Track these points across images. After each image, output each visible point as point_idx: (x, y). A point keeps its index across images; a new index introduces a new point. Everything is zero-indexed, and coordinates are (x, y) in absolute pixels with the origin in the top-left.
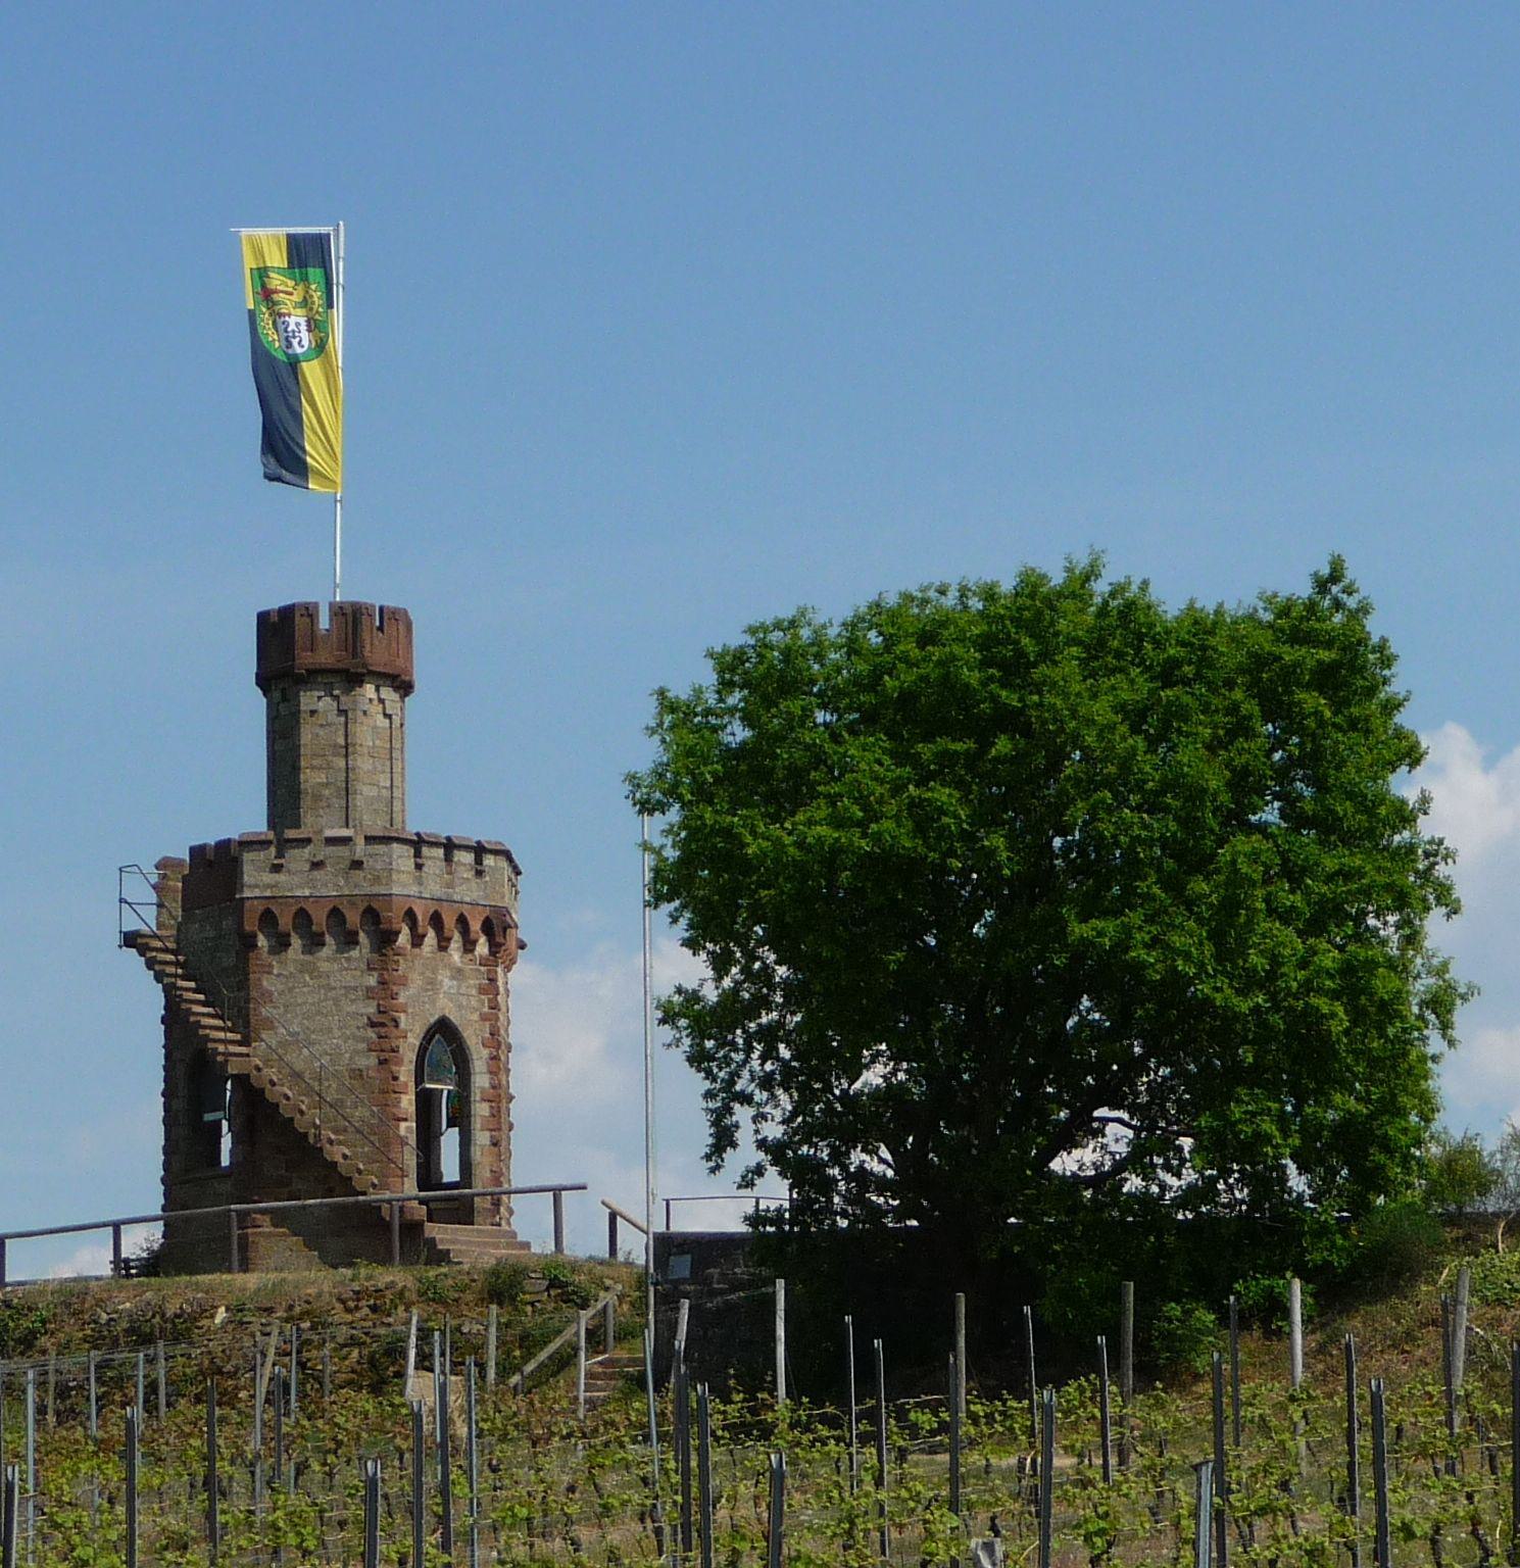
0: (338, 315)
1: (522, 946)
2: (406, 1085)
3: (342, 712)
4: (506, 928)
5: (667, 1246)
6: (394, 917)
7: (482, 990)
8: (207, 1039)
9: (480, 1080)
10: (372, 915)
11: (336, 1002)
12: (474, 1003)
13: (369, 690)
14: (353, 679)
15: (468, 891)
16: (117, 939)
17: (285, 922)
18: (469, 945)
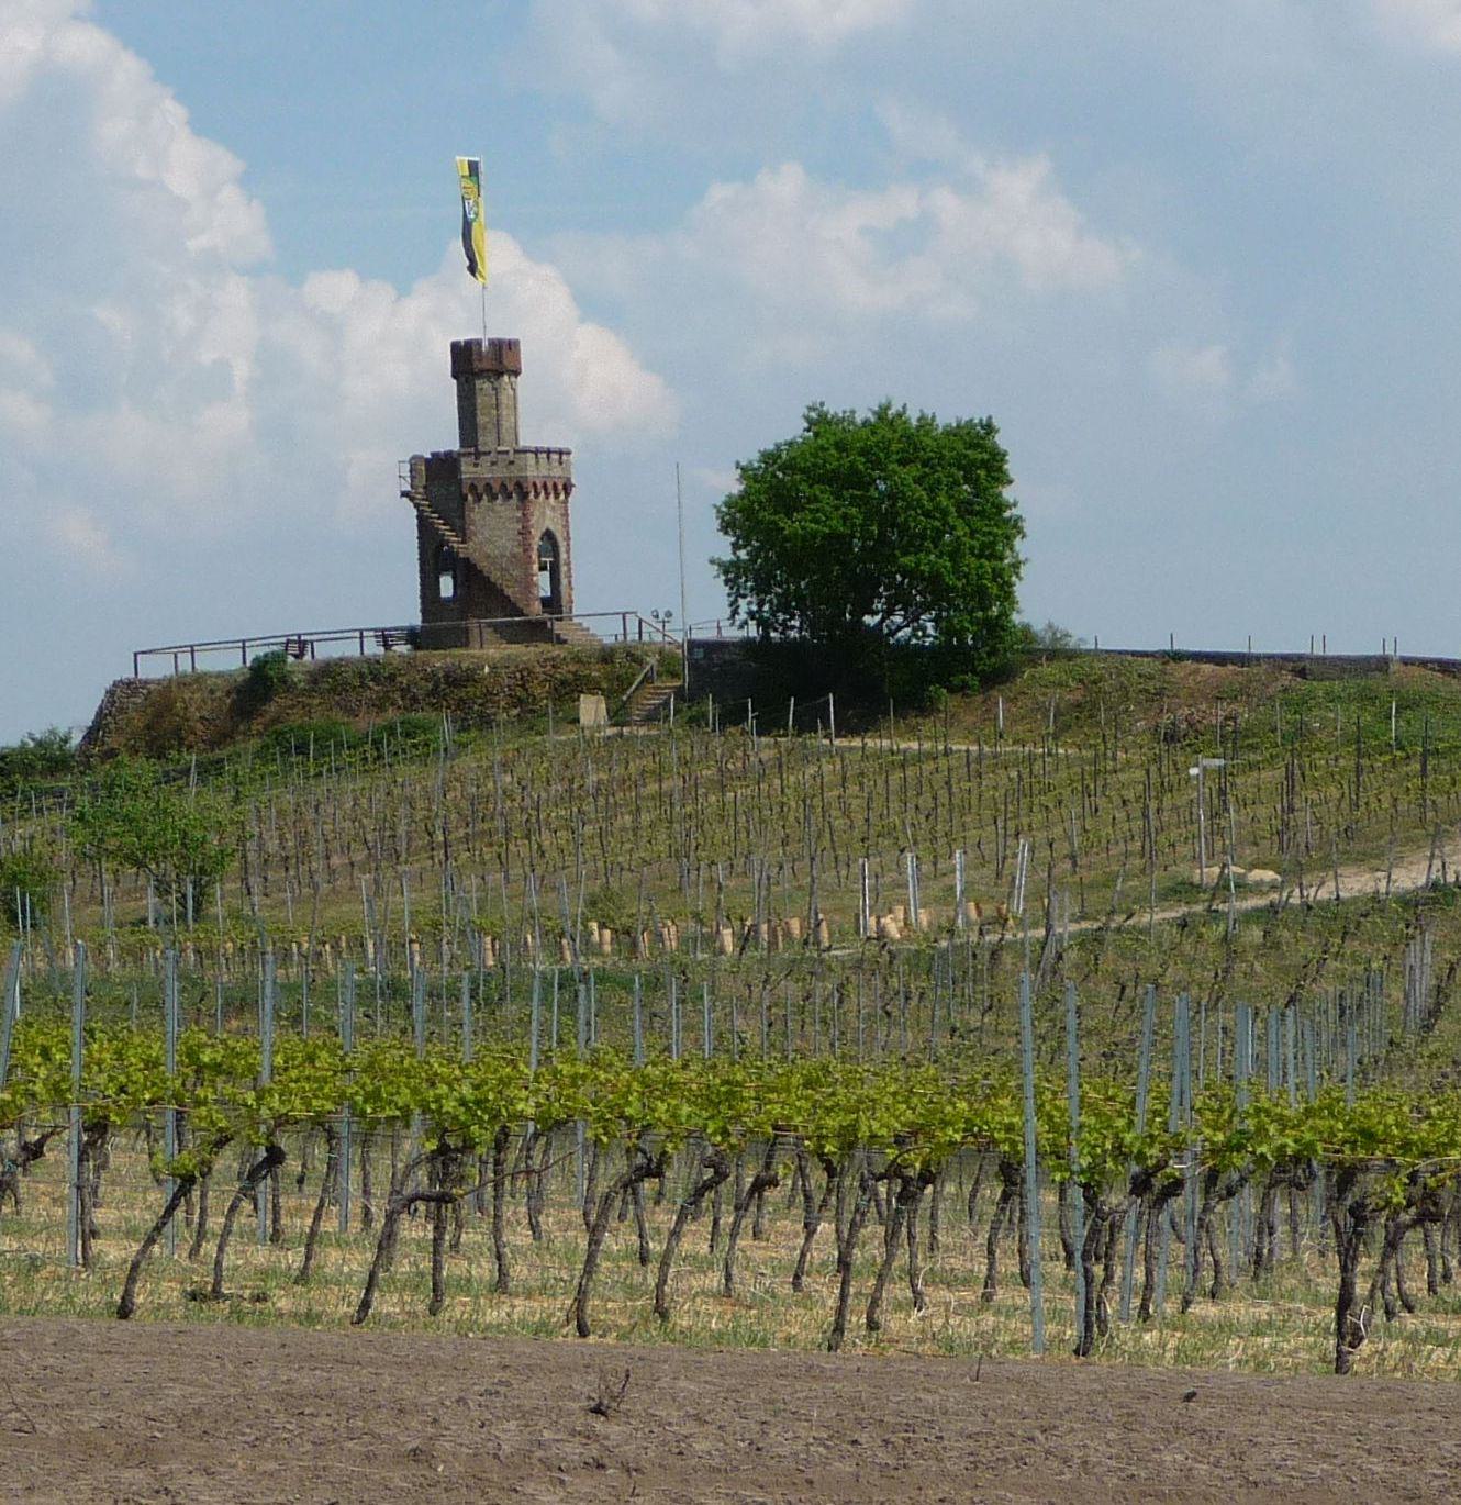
3: (495, 389)
5: (693, 645)
7: (562, 515)
9: (563, 556)
10: (519, 485)
14: (499, 374)
15: (557, 472)
17: (480, 489)
18: (557, 496)
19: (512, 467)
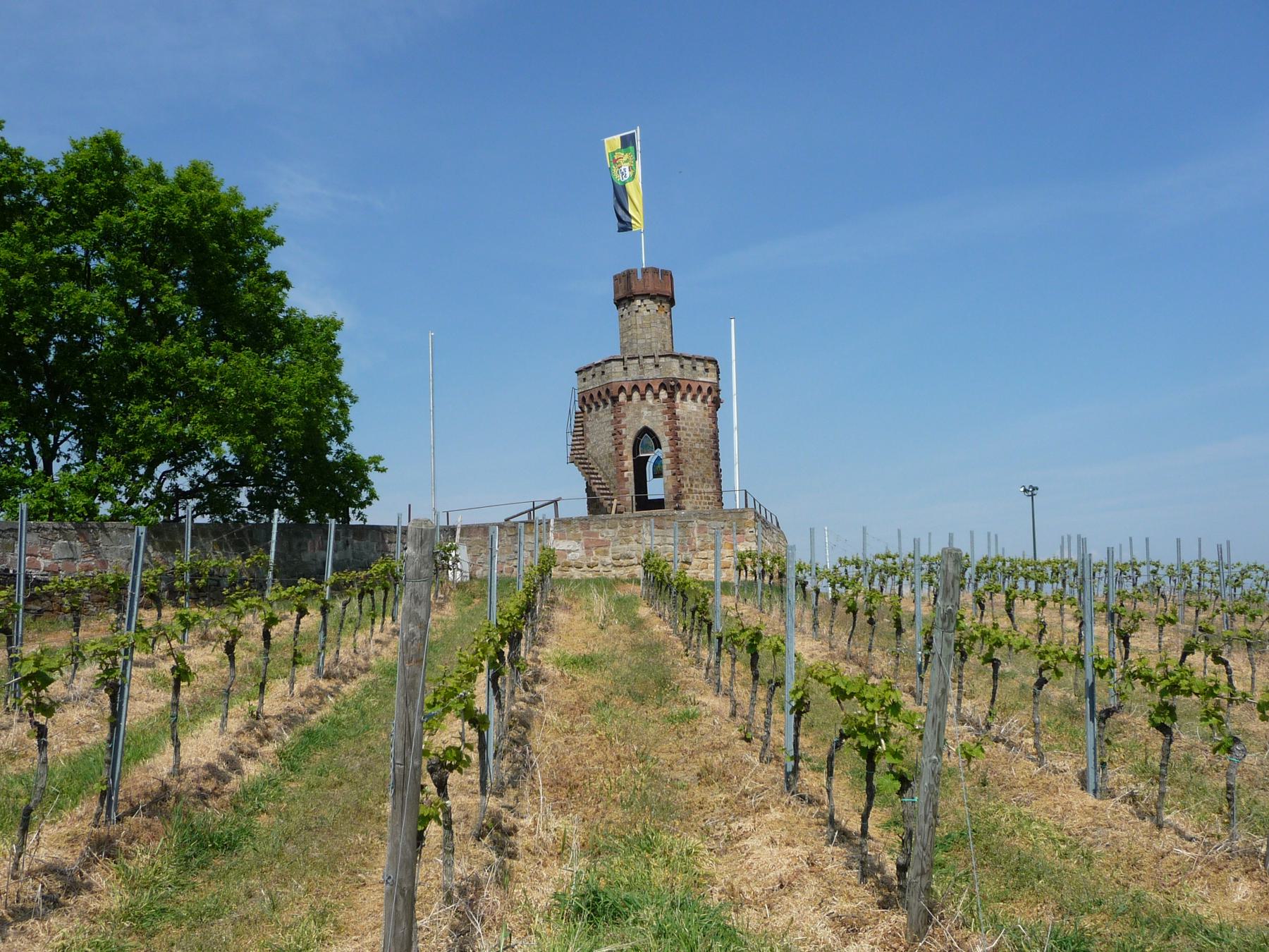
0: (638, 163)
18: (656, 396)
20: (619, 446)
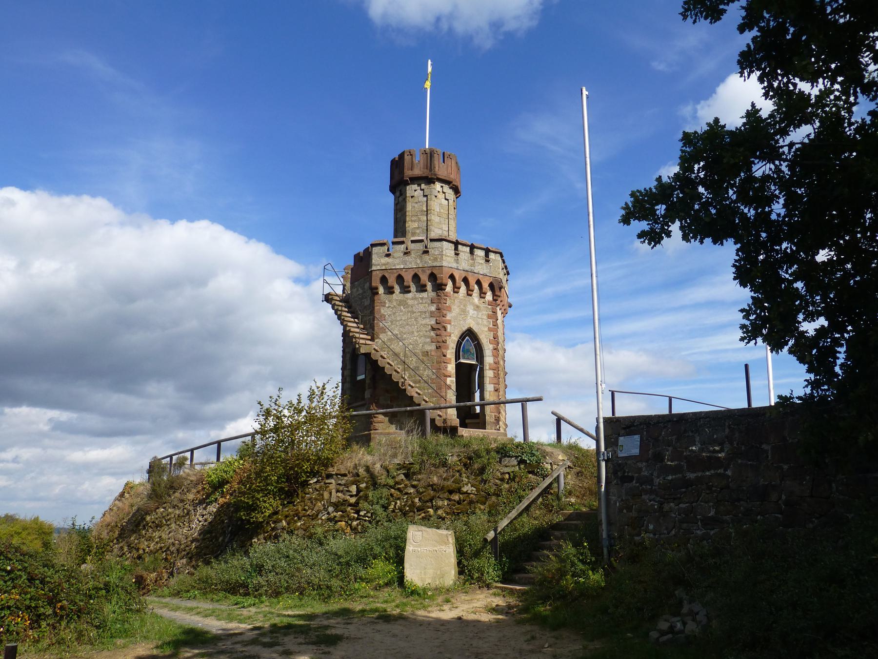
1: (510, 307)
2: (450, 359)
4: (501, 288)
5: (617, 427)
6: (444, 277)
7: (489, 317)
8: (353, 337)
9: (489, 359)
10: (433, 277)
11: (416, 319)
12: (485, 322)
13: (438, 186)
14: (429, 180)
16: (322, 297)
17: (392, 281)
18: (482, 294)
19: (426, 257)
20: (440, 346)
